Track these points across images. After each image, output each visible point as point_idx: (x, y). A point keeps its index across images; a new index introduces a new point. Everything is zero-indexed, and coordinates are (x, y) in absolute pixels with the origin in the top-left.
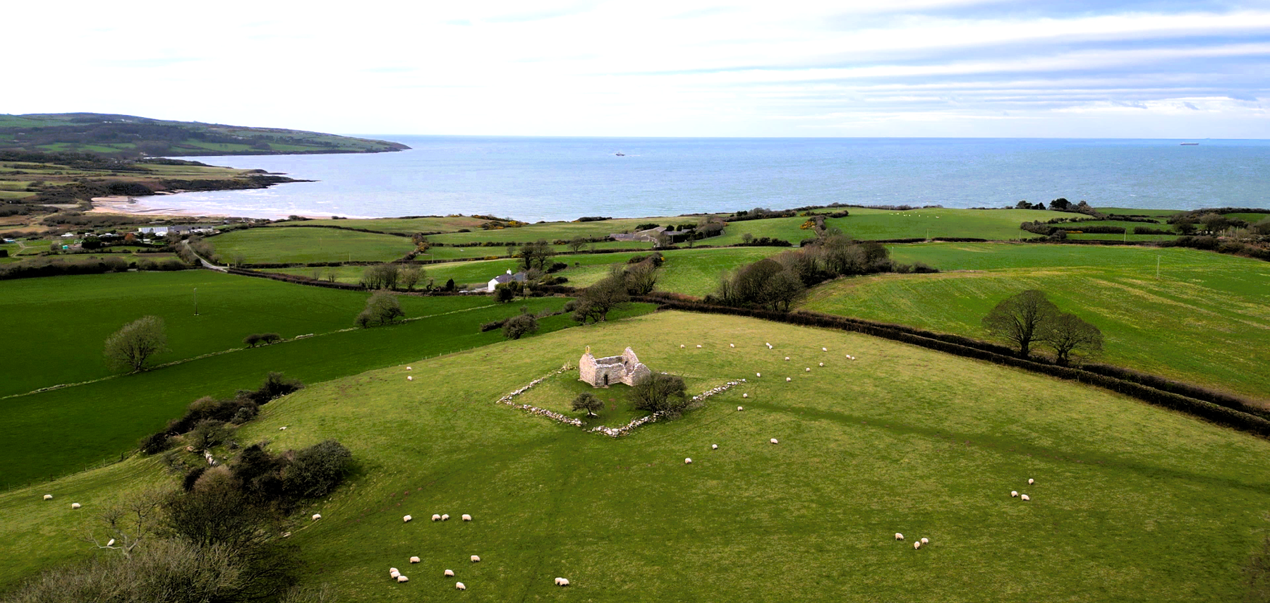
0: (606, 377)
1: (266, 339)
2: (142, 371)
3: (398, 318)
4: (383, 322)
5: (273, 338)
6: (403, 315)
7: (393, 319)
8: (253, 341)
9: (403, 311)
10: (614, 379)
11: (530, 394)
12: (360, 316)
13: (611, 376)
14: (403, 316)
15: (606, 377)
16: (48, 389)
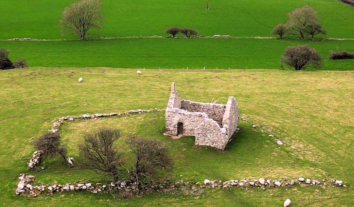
0: (180, 125)
1: (185, 32)
2: (84, 39)
3: (318, 36)
4: (302, 37)
5: (192, 33)
6: (324, 33)
7: (314, 36)
8: (174, 32)
9: (322, 29)
10: (191, 130)
11: (104, 120)
12: (277, 27)
13: (187, 125)
14: (324, 33)
15: (180, 125)
16: (20, 39)
